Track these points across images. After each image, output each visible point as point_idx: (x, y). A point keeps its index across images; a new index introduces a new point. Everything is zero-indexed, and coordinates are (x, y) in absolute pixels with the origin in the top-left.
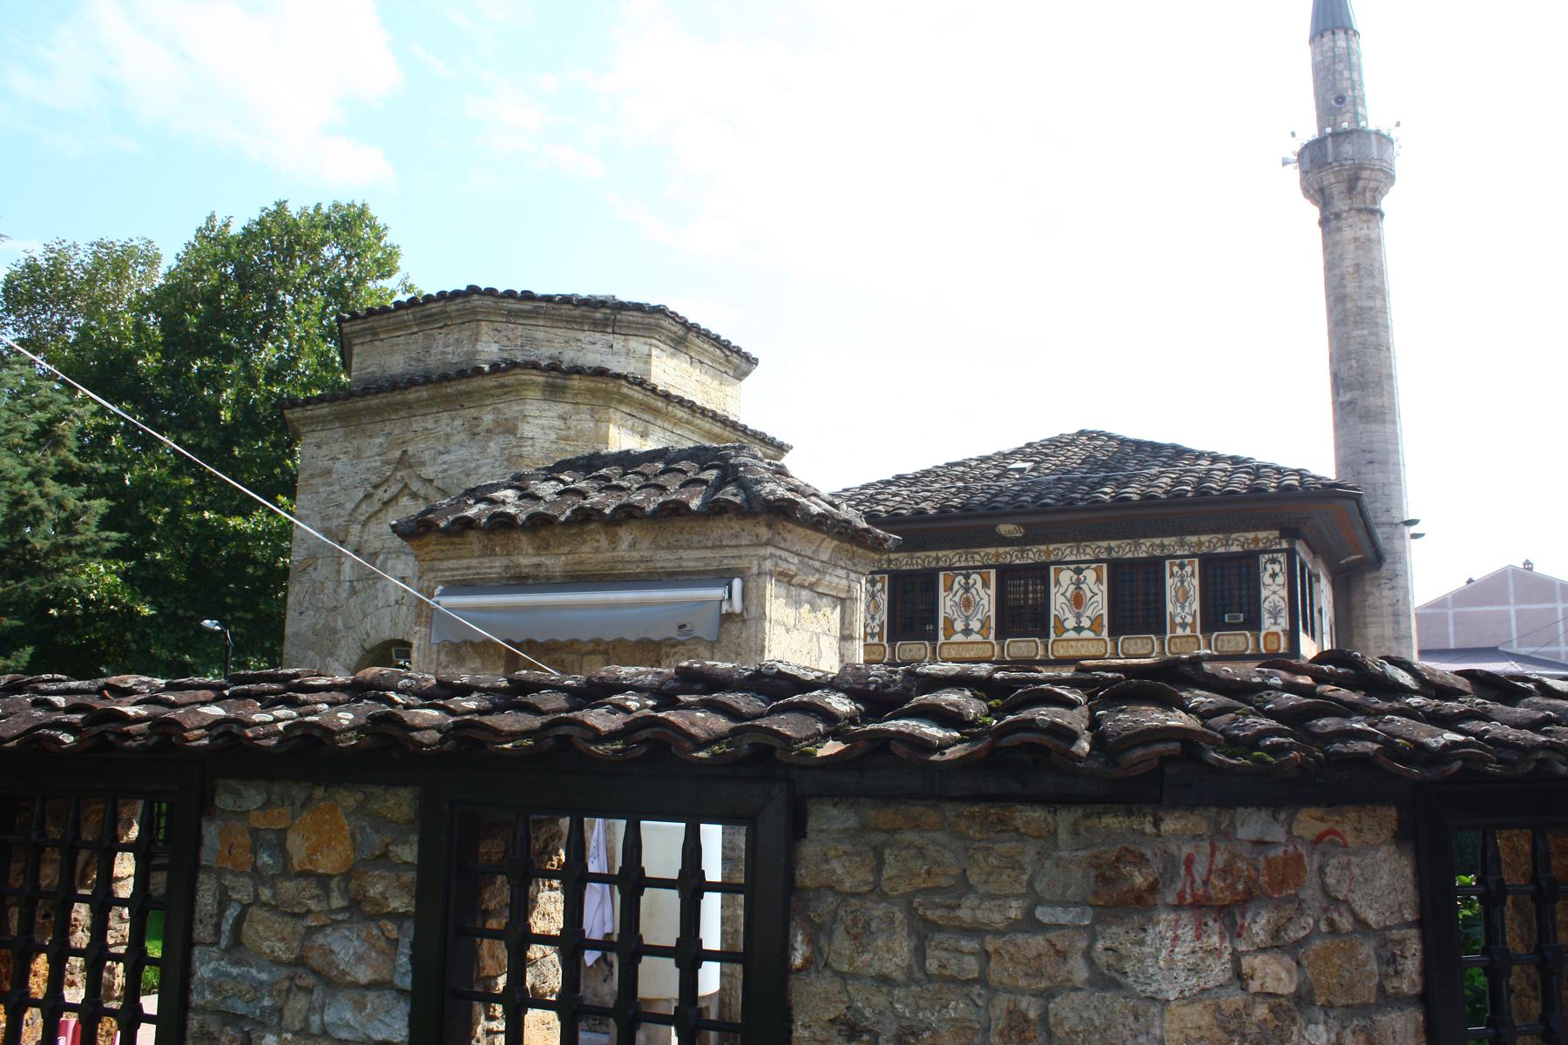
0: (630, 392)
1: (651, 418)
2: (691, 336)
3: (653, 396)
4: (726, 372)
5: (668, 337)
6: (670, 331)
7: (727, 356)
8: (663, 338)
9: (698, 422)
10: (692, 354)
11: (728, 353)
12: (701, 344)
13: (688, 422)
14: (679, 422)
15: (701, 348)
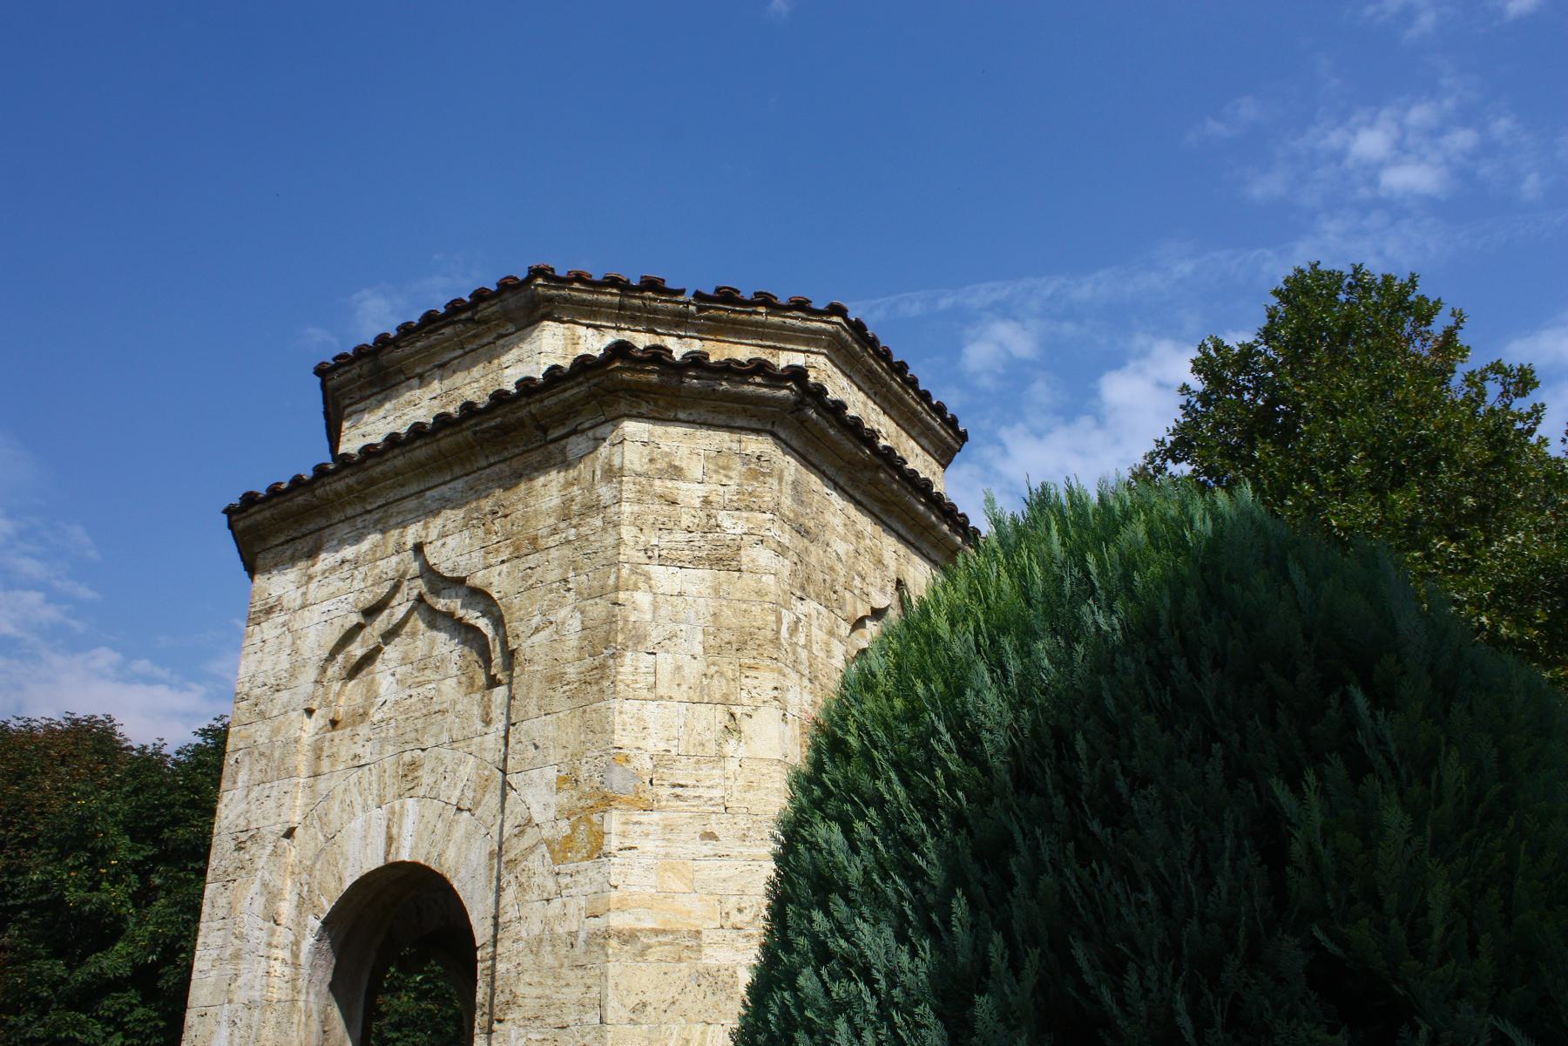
0: (248, 522)
1: (324, 523)
2: (385, 358)
3: (282, 499)
4: (501, 336)
5: (360, 388)
6: (352, 381)
7: (471, 320)
8: (357, 396)
9: (379, 469)
10: (419, 370)
11: (463, 316)
12: (408, 350)
13: (372, 482)
14: (359, 495)
15: (417, 352)
